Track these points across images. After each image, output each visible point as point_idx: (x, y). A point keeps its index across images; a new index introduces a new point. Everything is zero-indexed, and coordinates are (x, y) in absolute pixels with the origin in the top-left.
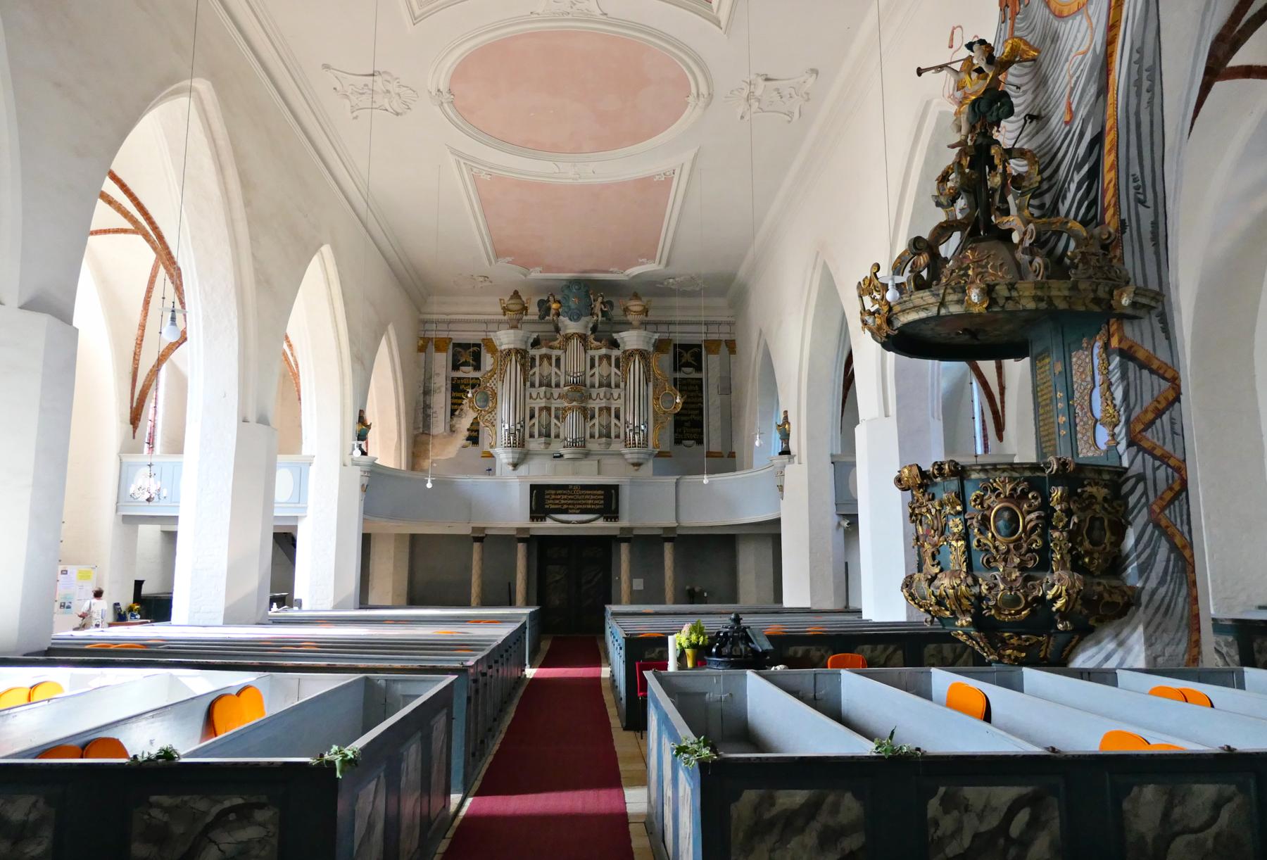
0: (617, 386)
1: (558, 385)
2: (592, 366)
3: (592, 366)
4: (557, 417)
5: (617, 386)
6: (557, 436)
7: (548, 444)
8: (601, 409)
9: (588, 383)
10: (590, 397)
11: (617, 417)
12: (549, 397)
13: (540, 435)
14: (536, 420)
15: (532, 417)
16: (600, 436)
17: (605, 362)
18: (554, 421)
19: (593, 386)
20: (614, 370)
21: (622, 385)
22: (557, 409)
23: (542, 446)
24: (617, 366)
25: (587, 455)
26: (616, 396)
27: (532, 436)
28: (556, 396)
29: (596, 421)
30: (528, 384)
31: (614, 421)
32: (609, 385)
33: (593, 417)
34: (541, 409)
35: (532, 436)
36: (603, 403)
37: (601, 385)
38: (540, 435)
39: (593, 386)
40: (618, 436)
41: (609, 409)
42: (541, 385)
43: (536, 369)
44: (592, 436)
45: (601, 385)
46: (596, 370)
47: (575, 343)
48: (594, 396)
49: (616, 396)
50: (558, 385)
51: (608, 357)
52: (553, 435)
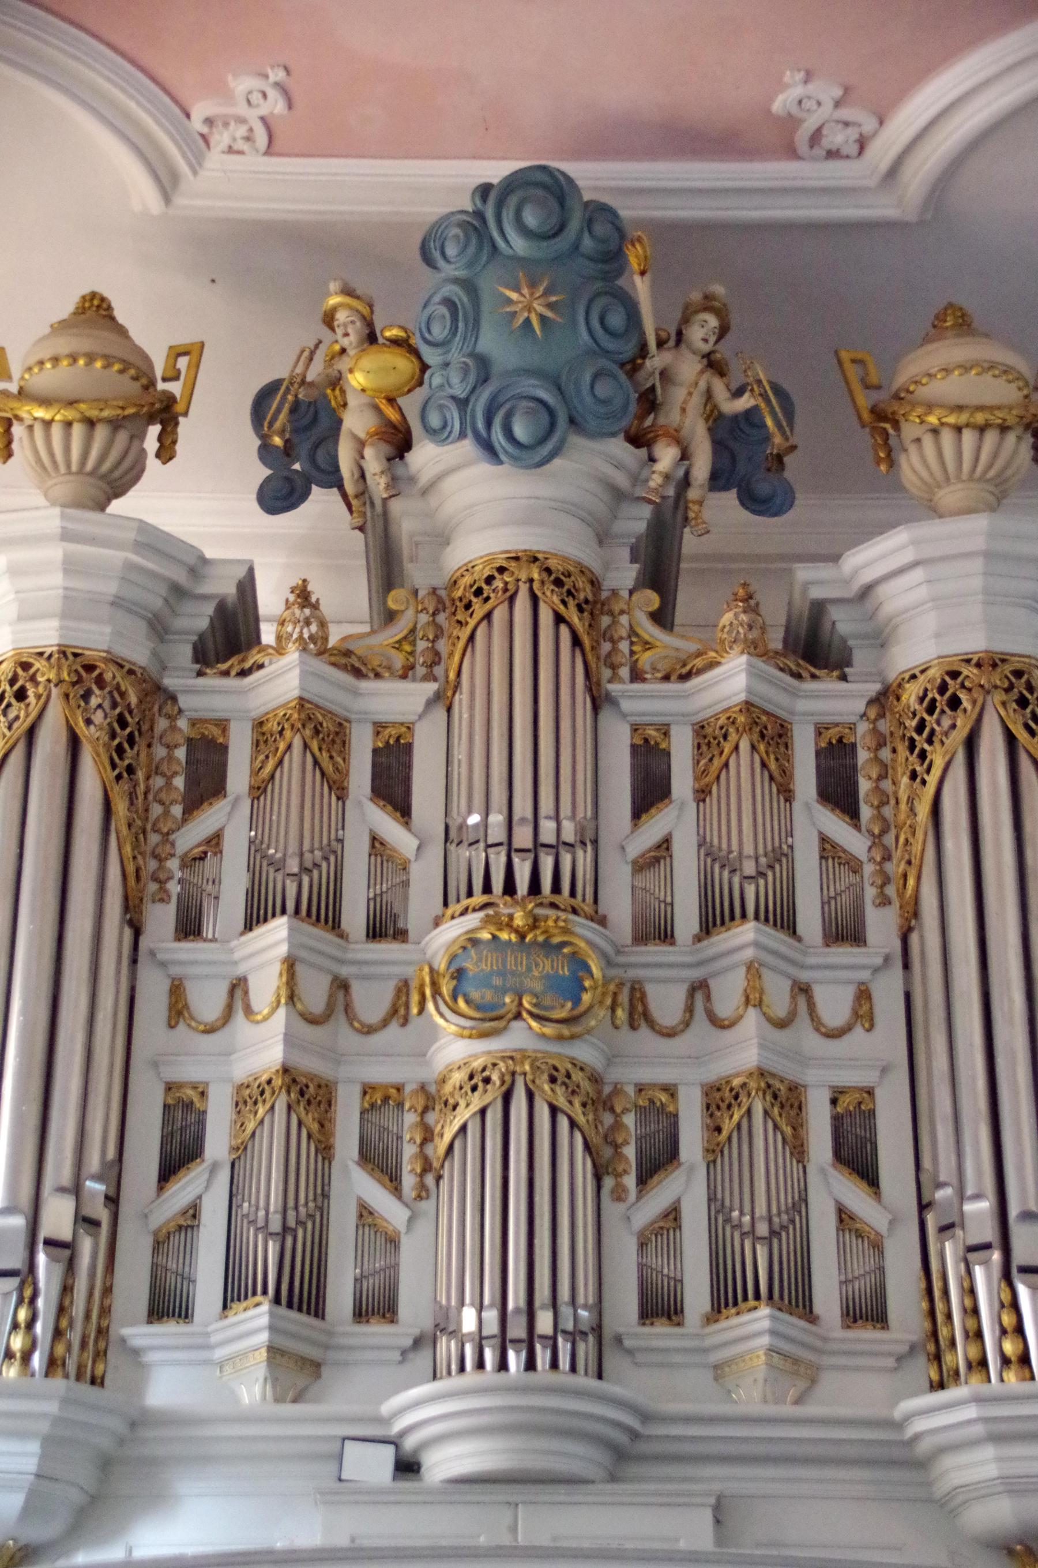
0: (846, 931)
1: (384, 927)
2: (650, 791)
3: (650, 791)
4: (379, 1161)
5: (846, 931)
6: (377, 1305)
7: (298, 1369)
8: (719, 1099)
9: (619, 903)
10: (639, 1014)
11: (858, 1159)
12: (325, 1005)
13: (235, 1292)
14: (204, 1187)
15: (179, 1155)
16: (727, 1296)
17: (744, 762)
18: (355, 1184)
19: (657, 930)
20: (813, 820)
21: (881, 926)
22: (380, 1100)
23: (251, 1388)
24: (839, 793)
25: (627, 1453)
26: (834, 1003)
27: (167, 1305)
28: (371, 1001)
29: (687, 1187)
30: (161, 919)
31: (830, 1187)
32: (783, 919)
33: (659, 1158)
34: (248, 1097)
35: (167, 1305)
36: (743, 1050)
37: (715, 917)
38: (235, 1292)
39: (657, 930)
40: (868, 1311)
41: (787, 1100)
42: (255, 917)
43: (229, 818)
44: (660, 1305)
45: (715, 917)
46: (677, 820)
47: (501, 656)
48: (667, 1002)
49: (834, 1003)
50: (384, 927)
51: (770, 732)
52: (340, 1295)
